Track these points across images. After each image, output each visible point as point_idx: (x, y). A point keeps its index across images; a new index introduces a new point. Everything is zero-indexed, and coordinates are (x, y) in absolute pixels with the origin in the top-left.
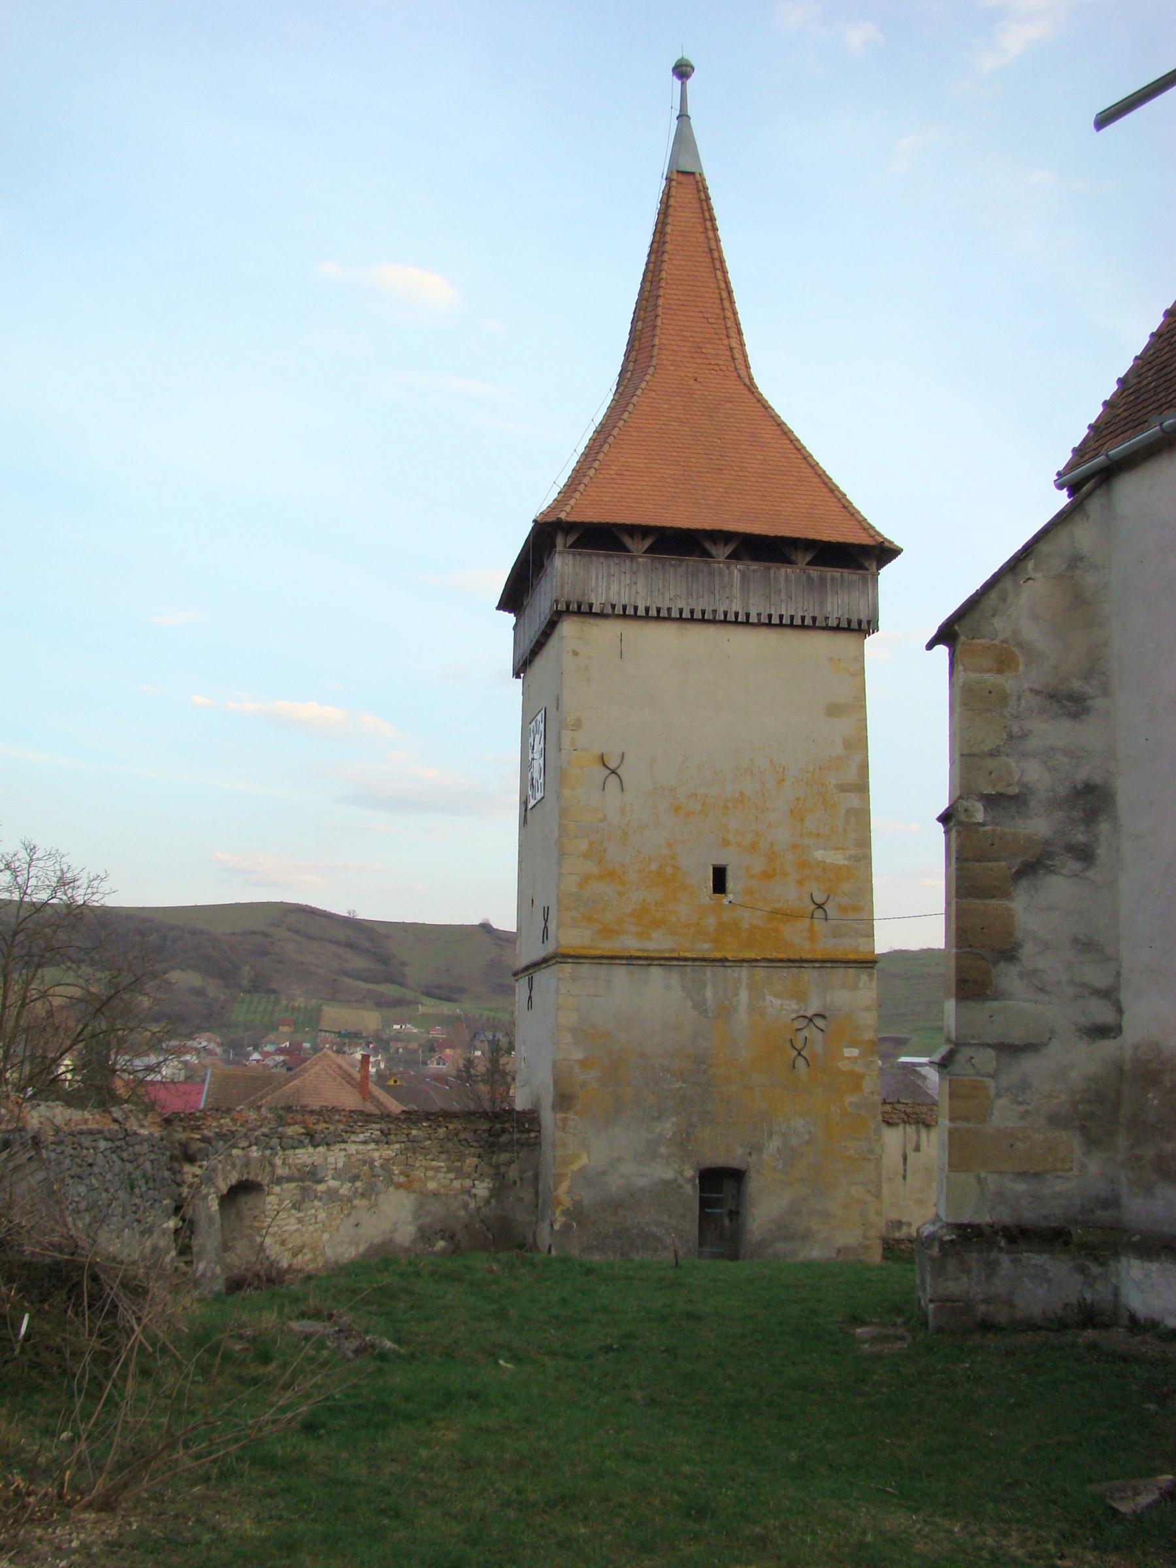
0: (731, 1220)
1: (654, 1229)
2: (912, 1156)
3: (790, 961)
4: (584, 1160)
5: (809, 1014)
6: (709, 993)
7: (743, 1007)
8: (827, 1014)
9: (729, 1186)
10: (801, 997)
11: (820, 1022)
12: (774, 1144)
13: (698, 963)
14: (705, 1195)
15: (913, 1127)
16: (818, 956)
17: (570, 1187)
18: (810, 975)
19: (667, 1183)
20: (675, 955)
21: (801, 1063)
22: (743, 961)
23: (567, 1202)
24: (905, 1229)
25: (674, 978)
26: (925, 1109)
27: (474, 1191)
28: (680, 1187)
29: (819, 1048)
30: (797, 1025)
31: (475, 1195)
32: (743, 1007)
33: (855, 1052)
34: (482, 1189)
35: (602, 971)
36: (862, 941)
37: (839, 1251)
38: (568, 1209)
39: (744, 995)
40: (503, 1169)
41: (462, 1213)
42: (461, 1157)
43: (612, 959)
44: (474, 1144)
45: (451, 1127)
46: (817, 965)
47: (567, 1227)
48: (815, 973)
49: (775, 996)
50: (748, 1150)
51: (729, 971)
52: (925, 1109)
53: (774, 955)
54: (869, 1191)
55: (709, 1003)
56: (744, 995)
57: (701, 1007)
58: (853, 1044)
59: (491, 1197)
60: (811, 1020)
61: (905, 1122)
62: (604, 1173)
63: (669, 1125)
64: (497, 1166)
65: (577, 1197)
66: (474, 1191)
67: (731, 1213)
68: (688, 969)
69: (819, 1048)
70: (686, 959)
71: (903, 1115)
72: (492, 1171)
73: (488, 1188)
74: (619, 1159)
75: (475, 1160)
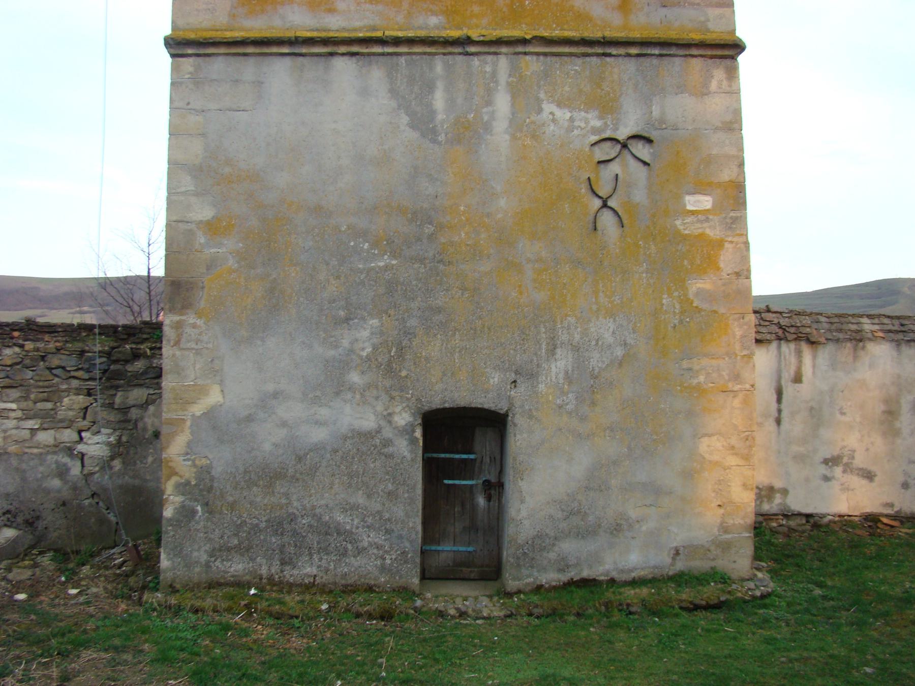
0: (489, 498)
1: (340, 518)
2: (789, 390)
3: (584, 42)
4: (214, 397)
5: (622, 134)
6: (439, 101)
7: (501, 126)
8: (653, 135)
9: (483, 443)
10: (608, 106)
11: (641, 150)
12: (561, 364)
13: (417, 49)
14: (429, 455)
15: (792, 346)
16: (636, 35)
17: (189, 444)
18: (622, 70)
19: (367, 436)
20: (379, 34)
21: (607, 218)
22: (499, 42)
23: (186, 470)
24: (778, 499)
25: (377, 74)
26: (807, 321)
27: (81, 448)
28: (387, 443)
29: (640, 196)
30: (601, 153)
31: (82, 456)
32: (501, 126)
33: (705, 202)
34: (95, 446)
35: (248, 69)
36: (713, 12)
37: (677, 553)
38: (188, 483)
39: (502, 103)
40: (134, 413)
41: (56, 483)
42: (53, 395)
43: (264, 44)
44: (80, 374)
45: (29, 345)
46: (634, 51)
47: (186, 513)
48: (630, 66)
49: (559, 105)
50: (513, 376)
51: (476, 61)
52: (807, 321)
53: (557, 33)
54: (733, 448)
55: (440, 117)
56: (502, 103)
57: (424, 124)
58: (700, 188)
59: (112, 458)
60: (625, 146)
61: (779, 339)
62: (249, 419)
63: (365, 334)
64: (124, 410)
65: (204, 462)
66: (81, 448)
67: (487, 485)
68: (402, 60)
69: (640, 196)
70: (397, 41)
71: (775, 329)
72: (113, 417)
73: (109, 444)
74: (275, 395)
75: (81, 400)
